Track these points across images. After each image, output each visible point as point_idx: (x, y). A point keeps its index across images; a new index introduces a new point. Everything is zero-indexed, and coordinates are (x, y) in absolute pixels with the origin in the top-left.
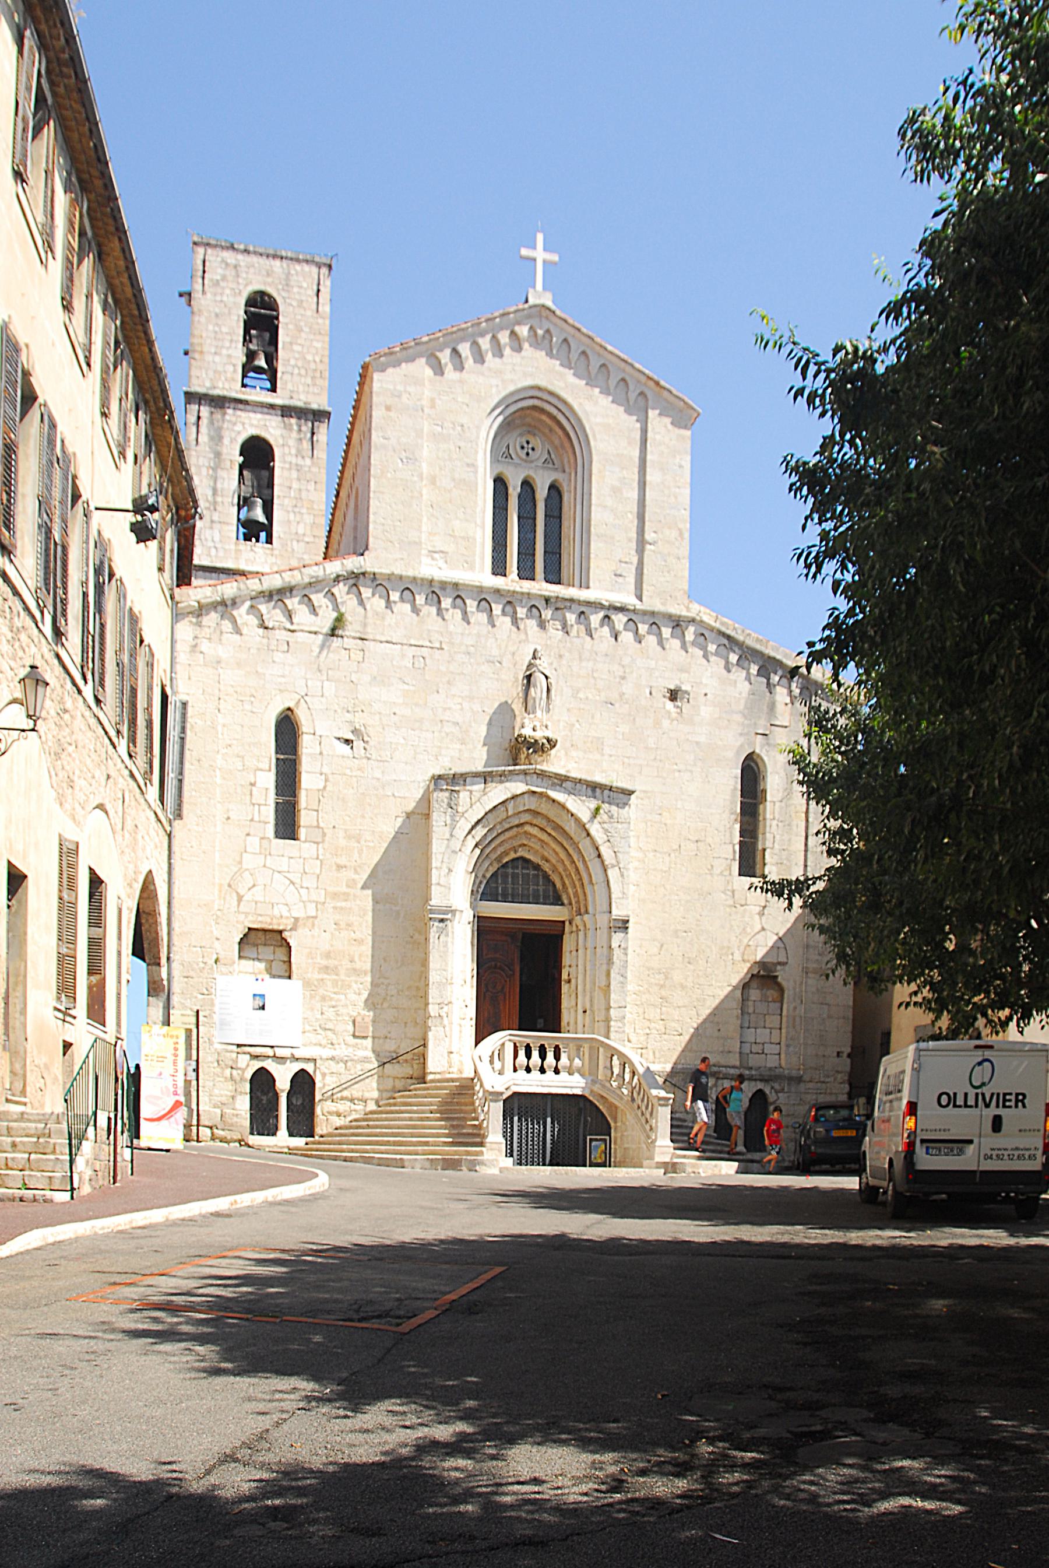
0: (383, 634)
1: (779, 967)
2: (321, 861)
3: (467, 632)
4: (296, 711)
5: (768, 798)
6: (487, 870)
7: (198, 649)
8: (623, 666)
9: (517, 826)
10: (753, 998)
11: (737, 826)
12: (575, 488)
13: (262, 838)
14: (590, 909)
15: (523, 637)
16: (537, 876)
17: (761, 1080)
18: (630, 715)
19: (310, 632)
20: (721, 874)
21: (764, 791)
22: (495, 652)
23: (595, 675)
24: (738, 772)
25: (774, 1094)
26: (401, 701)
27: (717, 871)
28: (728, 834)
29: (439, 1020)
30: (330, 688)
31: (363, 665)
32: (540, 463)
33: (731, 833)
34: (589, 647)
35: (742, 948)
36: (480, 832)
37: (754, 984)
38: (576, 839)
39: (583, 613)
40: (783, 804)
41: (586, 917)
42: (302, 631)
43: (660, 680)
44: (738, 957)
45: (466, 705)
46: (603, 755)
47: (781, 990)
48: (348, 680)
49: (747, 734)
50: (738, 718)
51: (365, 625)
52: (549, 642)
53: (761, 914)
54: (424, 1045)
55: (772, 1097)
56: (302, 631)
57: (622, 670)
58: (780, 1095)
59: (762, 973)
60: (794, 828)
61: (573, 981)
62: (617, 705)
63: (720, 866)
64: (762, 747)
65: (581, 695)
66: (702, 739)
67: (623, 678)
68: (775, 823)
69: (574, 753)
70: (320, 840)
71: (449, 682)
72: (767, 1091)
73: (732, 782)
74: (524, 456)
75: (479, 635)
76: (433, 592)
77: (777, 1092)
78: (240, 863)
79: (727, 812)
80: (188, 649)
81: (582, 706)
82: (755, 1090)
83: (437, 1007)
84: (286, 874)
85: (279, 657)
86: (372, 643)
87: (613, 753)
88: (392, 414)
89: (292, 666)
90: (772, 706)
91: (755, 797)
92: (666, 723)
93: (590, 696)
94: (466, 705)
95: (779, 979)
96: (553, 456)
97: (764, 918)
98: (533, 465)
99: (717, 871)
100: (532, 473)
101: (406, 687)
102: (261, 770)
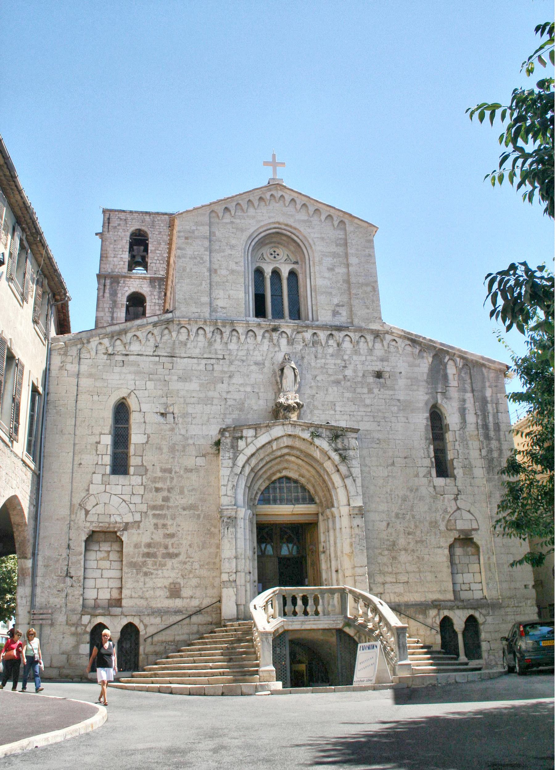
0: (185, 353)
1: (473, 532)
2: (145, 486)
3: (241, 348)
4: (128, 399)
5: (450, 429)
6: (261, 485)
7: (64, 368)
8: (345, 361)
9: (281, 456)
10: (458, 554)
11: (432, 447)
12: (306, 271)
13: (103, 475)
14: (335, 505)
15: (277, 349)
16: (297, 486)
17: (471, 609)
18: (351, 386)
19: (138, 355)
20: (424, 477)
21: (447, 426)
22: (259, 358)
23: (326, 367)
24: (427, 415)
25: (482, 617)
26: (198, 389)
27: (421, 475)
28: (426, 452)
29: (229, 584)
30: (150, 385)
31: (173, 370)
32: (282, 261)
33: (428, 451)
34: (321, 352)
35: (446, 521)
36: (253, 462)
37: (457, 545)
38: (321, 461)
39: (315, 333)
40: (461, 432)
41: (333, 509)
42: (133, 355)
43: (369, 367)
44: (443, 527)
45: (242, 389)
46: (335, 411)
47: (477, 547)
48: (162, 379)
49: (431, 393)
50: (424, 383)
51: (174, 349)
52: (294, 351)
53: (456, 499)
54: (220, 601)
55: (481, 619)
56: (133, 355)
57: (343, 362)
58: (487, 617)
59: (462, 537)
60: (470, 446)
61: (328, 552)
62: (343, 383)
63: (422, 471)
64: (442, 399)
65: (318, 378)
66: (402, 398)
67: (345, 367)
68: (457, 443)
69: (316, 412)
70: (143, 473)
71: (230, 377)
72: (477, 615)
73: (425, 422)
74: (273, 258)
75: (248, 350)
76: (218, 329)
77: (484, 616)
78: (88, 490)
79: (423, 438)
80: (57, 368)
81: (319, 384)
82: (468, 615)
83: (227, 575)
84: (121, 496)
85: (116, 370)
86: (178, 359)
87: (342, 410)
88: (189, 241)
89: (126, 374)
90: (445, 377)
91: (441, 429)
92: (376, 391)
93: (324, 379)
94: (242, 389)
95: (475, 540)
96: (290, 257)
97: (458, 502)
98: (279, 262)
99: (421, 475)
100: (277, 265)
101: (201, 382)
102: (104, 434)
